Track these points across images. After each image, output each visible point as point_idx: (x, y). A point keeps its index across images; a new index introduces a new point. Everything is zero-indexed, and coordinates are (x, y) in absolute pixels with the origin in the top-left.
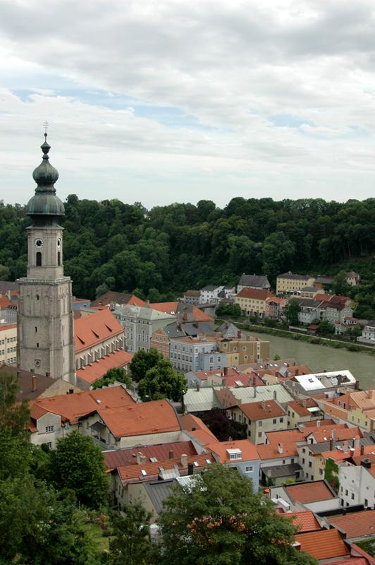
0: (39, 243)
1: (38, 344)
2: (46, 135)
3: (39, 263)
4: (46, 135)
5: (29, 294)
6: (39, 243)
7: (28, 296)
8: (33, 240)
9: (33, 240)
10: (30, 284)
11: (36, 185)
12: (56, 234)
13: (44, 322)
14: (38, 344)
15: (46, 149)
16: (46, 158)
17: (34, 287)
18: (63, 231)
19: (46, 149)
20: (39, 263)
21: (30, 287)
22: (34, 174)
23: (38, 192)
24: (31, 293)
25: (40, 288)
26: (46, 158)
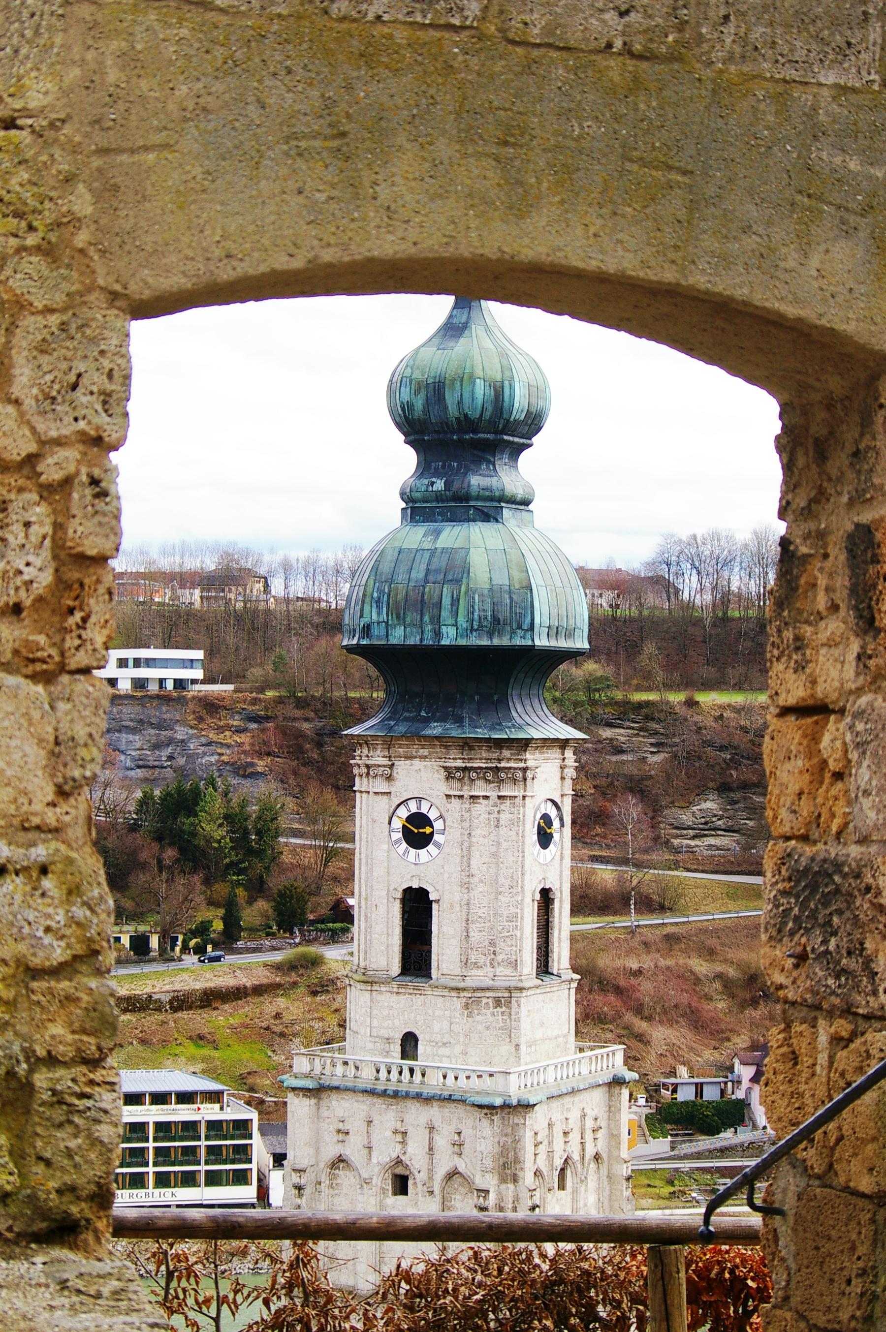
3: (416, 958)
6: (418, 831)
9: (383, 806)
11: (405, 460)
12: (523, 776)
18: (579, 748)
20: (416, 958)
22: (392, 390)
23: (419, 508)
25: (417, 1116)
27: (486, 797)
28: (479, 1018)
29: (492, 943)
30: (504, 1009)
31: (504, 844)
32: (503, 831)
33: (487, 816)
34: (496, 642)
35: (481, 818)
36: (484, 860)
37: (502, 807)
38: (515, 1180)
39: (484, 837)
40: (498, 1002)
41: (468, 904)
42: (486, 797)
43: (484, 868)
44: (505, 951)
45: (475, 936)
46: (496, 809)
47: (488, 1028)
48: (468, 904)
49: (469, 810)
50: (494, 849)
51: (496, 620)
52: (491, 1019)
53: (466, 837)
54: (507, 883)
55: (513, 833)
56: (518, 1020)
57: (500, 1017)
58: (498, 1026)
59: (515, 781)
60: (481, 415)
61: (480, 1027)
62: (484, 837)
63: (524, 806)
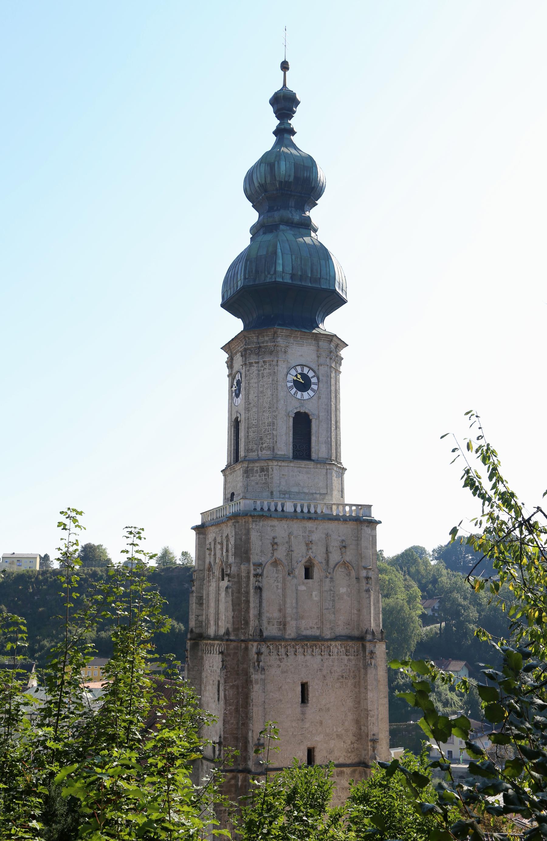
0: (303, 384)
1: (311, 753)
2: (285, 66)
4: (285, 66)
5: (280, 554)
7: (276, 563)
8: (282, 368)
10: (283, 516)
13: (338, 660)
14: (311, 753)
15: (284, 104)
16: (284, 133)
17: (296, 527)
19: (284, 104)
21: (280, 529)
24: (290, 551)
26: (284, 133)
27: (256, 363)
28: (252, 478)
29: (261, 439)
30: (265, 473)
31: (266, 386)
32: (265, 379)
33: (257, 372)
34: (257, 282)
35: (254, 374)
36: (255, 395)
37: (265, 367)
38: (248, 560)
39: (255, 383)
40: (262, 470)
41: (248, 419)
42: (258, 363)
43: (256, 399)
44: (267, 442)
45: (251, 434)
46: (262, 368)
47: (257, 483)
48: (248, 419)
49: (248, 371)
50: (261, 389)
51: (257, 271)
52: (259, 478)
53: (247, 385)
54: (267, 406)
55: (271, 379)
56: (272, 478)
57: (264, 478)
58: (262, 482)
59: (271, 353)
60: (266, 181)
61: (253, 483)
62: (255, 383)
63: (277, 365)
